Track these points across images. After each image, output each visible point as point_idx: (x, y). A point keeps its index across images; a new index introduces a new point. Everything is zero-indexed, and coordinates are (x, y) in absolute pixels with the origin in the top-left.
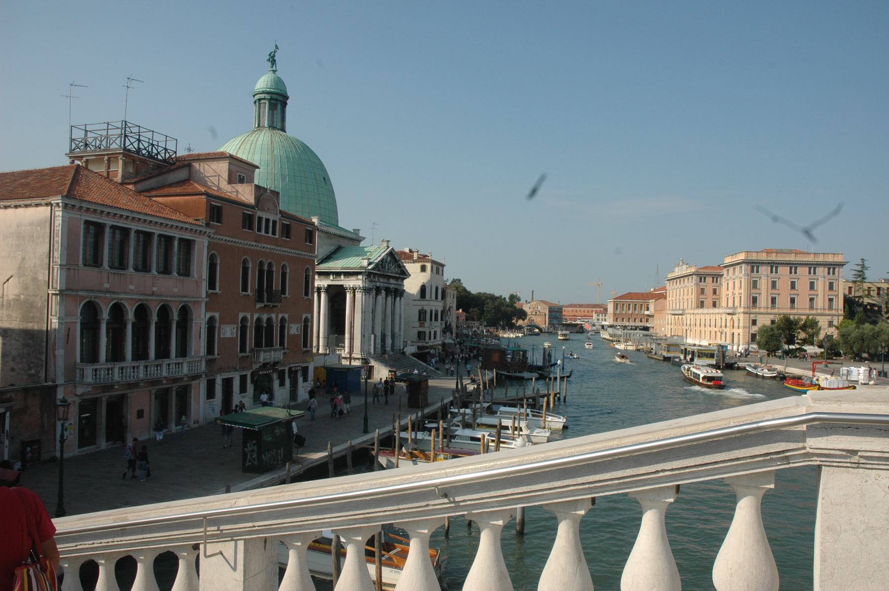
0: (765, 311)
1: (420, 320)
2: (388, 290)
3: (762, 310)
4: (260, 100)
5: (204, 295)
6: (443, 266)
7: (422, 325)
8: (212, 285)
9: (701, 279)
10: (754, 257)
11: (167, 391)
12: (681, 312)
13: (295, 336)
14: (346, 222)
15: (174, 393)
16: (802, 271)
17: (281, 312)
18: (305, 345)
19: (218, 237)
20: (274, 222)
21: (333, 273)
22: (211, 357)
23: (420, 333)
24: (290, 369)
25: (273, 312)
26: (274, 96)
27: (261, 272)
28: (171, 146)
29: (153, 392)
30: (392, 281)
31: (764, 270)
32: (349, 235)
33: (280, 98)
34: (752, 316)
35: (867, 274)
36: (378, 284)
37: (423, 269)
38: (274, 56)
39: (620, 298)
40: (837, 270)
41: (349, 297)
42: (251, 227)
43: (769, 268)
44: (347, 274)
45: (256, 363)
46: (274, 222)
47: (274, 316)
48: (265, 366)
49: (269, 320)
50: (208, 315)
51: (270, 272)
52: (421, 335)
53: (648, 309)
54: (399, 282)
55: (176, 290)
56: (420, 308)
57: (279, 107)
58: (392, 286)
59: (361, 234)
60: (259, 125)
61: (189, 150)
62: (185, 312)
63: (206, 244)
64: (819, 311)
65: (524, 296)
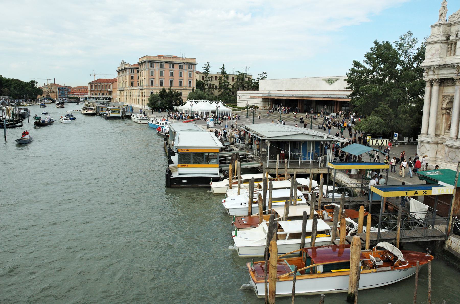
9: (131, 70)
12: (122, 89)
16: (167, 66)
53: (110, 88)
64: (184, 88)
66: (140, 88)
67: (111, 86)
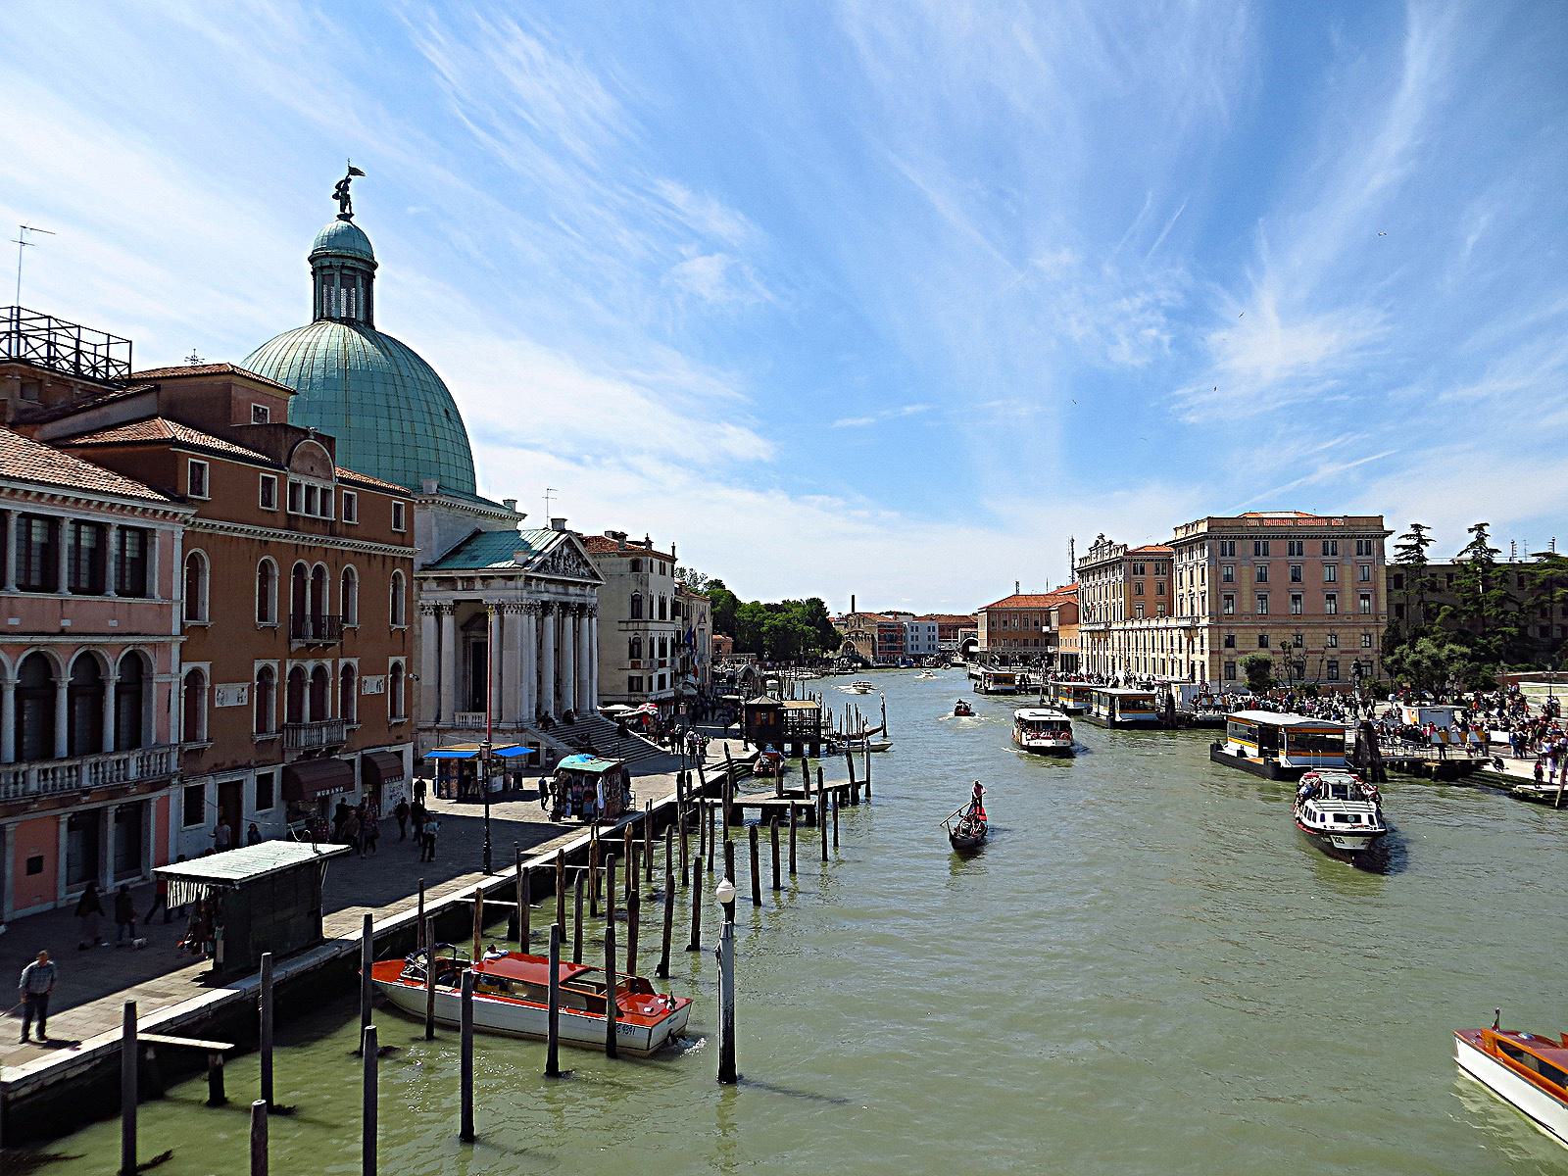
1: (631, 656)
2: (565, 607)
5: (176, 629)
8: (192, 612)
11: (98, 815)
13: (372, 696)
15: (111, 817)
19: (205, 522)
22: (194, 746)
23: (631, 679)
26: (349, 263)
28: (119, 353)
29: (64, 819)
30: (571, 589)
33: (361, 266)
35: (1427, 552)
36: (546, 597)
41: (493, 618)
47: (328, 663)
49: (319, 671)
50: (187, 668)
55: (113, 623)
58: (572, 599)
61: (193, 359)
62: (136, 666)
63: (179, 536)
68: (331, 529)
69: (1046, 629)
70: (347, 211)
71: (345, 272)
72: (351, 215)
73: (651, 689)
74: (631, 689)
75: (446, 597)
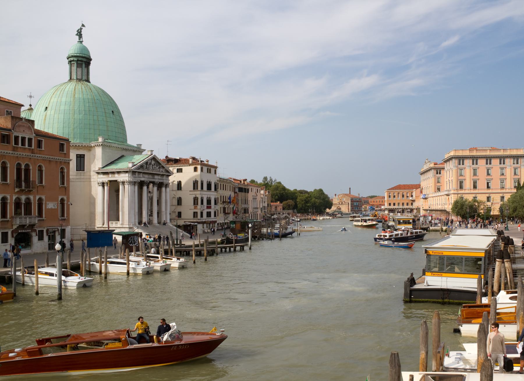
0: (469, 192)
1: (194, 204)
2: (153, 183)
3: (467, 192)
4: (71, 61)
6: (216, 167)
7: (195, 208)
10: (460, 153)
13: (52, 209)
14: (132, 141)
16: (482, 162)
17: (38, 194)
18: (63, 215)
20: (30, 140)
21: (111, 172)
23: (194, 213)
24: (47, 230)
25: (30, 194)
26: (80, 59)
27: (19, 170)
30: (156, 177)
31: (468, 162)
32: (135, 149)
34: (459, 195)
36: (143, 179)
37: (195, 169)
38: (81, 32)
39: (392, 189)
40: (519, 160)
42: (8, 142)
43: (471, 161)
44: (119, 173)
45: (15, 225)
46: (30, 140)
47: (32, 197)
48: (22, 226)
51: (27, 170)
52: (195, 214)
53: (412, 196)
54: (165, 177)
56: (194, 196)
57: (84, 65)
59: (143, 147)
60: (71, 78)
65: (329, 192)
66: (446, 193)
67: (414, 194)
68: (33, 152)
69: (411, 198)
70: (81, 40)
71: (79, 62)
72: (82, 42)
73: (202, 216)
74: (194, 217)
75: (105, 179)
